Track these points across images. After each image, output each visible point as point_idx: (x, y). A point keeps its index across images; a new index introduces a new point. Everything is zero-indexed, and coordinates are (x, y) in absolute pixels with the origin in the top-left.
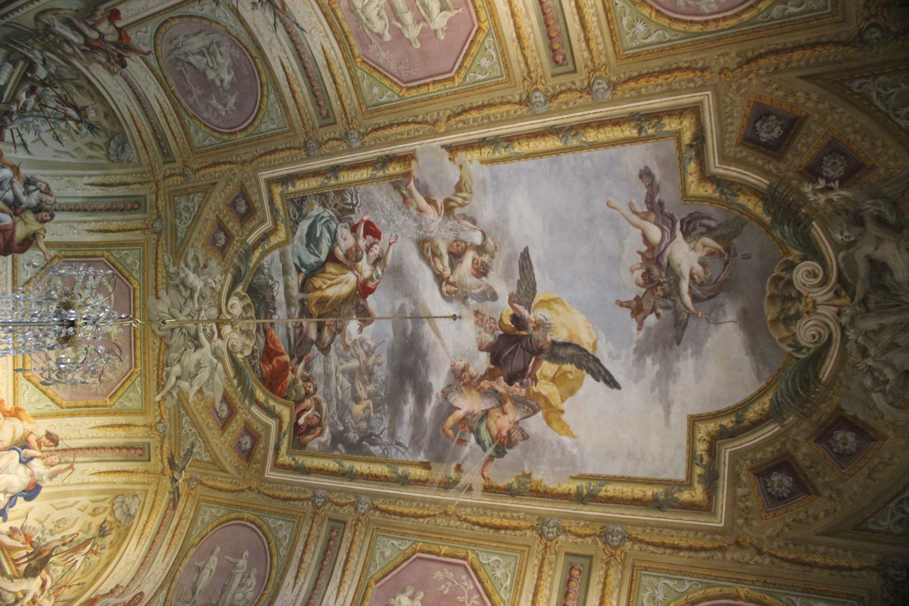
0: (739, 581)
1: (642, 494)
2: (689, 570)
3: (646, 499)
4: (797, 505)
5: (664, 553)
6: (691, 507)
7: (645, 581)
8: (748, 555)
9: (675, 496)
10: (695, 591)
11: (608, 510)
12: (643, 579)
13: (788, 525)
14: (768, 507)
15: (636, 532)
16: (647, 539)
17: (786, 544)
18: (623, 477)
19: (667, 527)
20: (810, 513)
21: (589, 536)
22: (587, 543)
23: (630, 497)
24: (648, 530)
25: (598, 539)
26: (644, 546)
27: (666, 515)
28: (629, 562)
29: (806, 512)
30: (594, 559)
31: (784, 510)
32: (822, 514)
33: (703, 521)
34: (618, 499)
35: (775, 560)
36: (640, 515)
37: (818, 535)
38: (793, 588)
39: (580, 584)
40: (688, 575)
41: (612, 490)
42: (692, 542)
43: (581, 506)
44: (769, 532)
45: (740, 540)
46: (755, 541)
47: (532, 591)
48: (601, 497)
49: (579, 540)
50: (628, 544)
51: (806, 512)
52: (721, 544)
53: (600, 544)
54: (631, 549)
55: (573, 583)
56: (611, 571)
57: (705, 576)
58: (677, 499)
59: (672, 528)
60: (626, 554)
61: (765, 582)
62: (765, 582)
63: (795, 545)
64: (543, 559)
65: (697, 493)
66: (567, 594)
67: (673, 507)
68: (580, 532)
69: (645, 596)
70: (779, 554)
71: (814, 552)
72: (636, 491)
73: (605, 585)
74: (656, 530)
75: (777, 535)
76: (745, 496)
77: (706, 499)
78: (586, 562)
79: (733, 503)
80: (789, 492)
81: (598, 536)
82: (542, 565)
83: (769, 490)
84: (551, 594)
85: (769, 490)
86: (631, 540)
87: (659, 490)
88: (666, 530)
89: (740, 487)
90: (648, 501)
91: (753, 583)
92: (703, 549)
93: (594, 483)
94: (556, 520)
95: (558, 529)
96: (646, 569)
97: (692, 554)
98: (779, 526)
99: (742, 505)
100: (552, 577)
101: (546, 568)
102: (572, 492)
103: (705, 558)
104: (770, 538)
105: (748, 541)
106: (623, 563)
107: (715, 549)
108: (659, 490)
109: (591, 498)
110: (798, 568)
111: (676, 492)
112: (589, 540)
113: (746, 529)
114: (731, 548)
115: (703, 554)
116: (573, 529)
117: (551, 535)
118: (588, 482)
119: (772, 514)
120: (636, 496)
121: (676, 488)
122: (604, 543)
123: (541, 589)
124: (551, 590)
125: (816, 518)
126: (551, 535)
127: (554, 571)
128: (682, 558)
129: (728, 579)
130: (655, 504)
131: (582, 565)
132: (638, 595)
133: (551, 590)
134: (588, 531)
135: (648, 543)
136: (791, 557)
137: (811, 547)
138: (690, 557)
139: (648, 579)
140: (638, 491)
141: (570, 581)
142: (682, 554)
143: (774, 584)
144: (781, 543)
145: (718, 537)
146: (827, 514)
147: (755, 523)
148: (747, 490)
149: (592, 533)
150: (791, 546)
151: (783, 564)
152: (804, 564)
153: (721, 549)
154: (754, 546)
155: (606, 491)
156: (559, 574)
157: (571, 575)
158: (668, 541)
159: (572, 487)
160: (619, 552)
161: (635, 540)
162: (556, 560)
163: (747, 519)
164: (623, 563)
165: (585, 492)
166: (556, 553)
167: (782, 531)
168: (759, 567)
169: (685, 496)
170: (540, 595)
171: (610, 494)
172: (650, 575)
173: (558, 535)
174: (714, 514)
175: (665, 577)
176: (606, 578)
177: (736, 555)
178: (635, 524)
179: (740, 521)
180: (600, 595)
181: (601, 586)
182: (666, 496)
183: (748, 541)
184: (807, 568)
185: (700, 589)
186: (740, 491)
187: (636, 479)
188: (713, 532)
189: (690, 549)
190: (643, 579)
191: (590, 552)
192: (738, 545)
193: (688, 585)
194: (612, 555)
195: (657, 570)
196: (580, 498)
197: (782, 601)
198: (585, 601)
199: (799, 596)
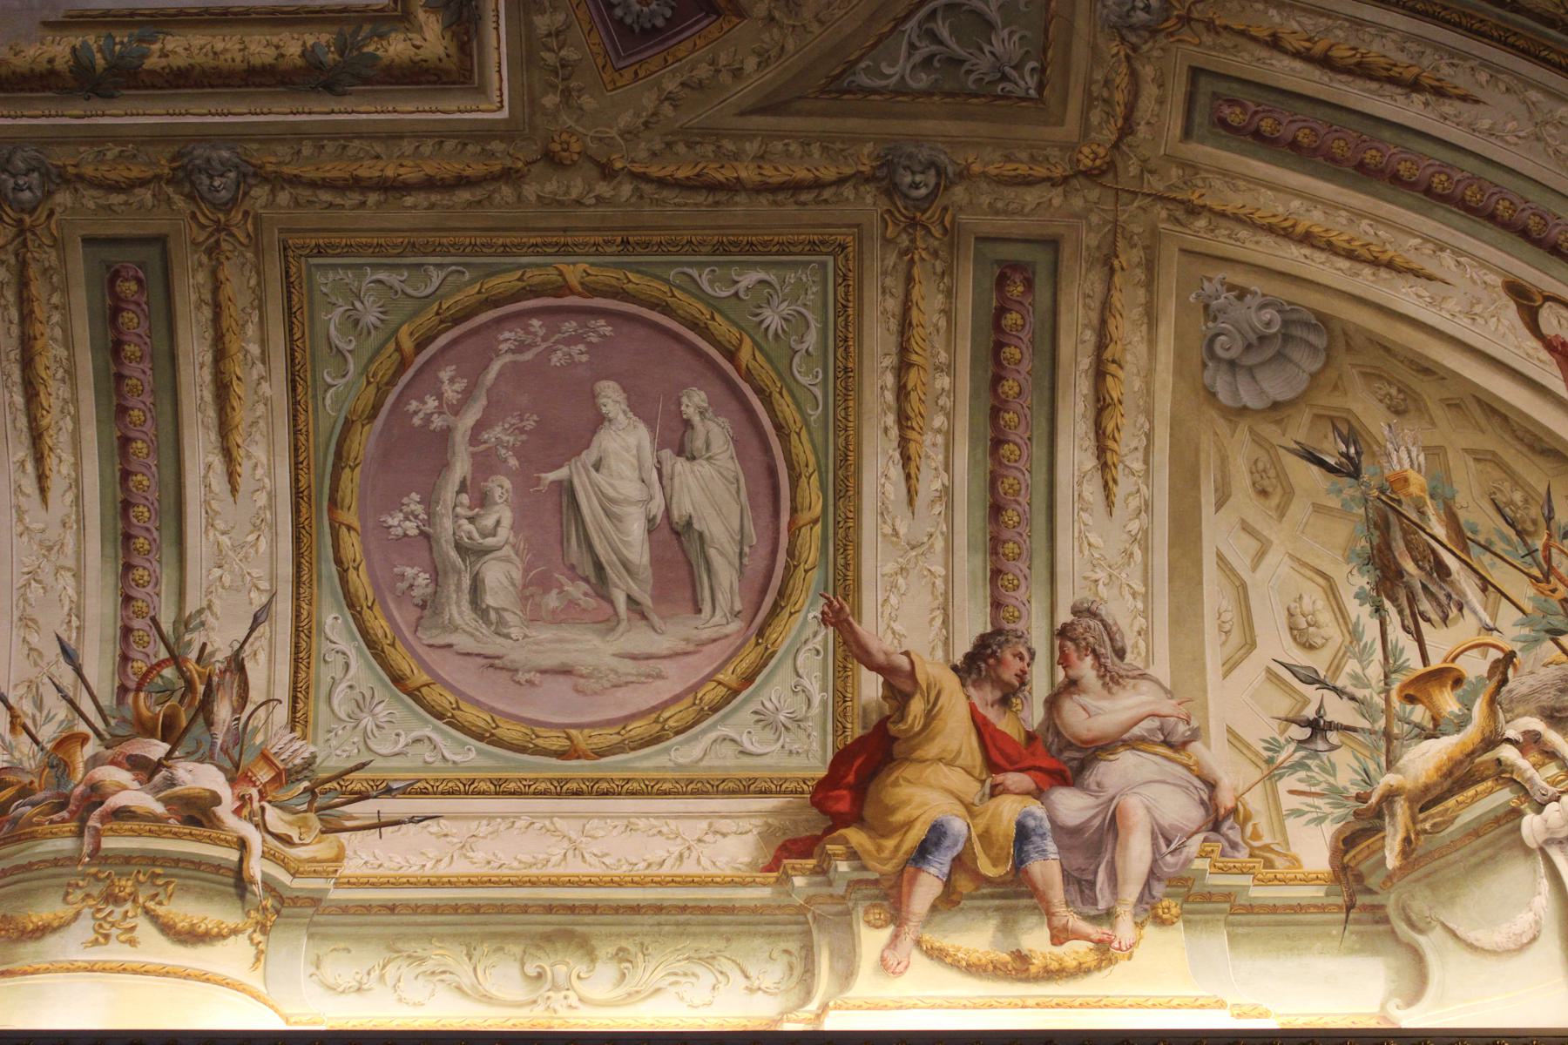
0: (563, 250)
1: (272, 52)
2: (433, 238)
3: (283, 64)
4: (689, 44)
5: (363, 204)
6: (416, 77)
7: (325, 281)
8: (579, 182)
9: (370, 49)
10: (459, 289)
11: (182, 106)
12: (319, 278)
13: (669, 98)
14: (619, 57)
15: (274, 158)
16: (310, 173)
17: (669, 145)
18: (206, 11)
19: (360, 136)
20: (723, 60)
21: (143, 183)
22: (141, 205)
23: (239, 64)
24: (307, 150)
25: (170, 190)
26: (305, 194)
27: (348, 103)
28: (272, 237)
29: (713, 63)
30: (171, 245)
31: (658, 60)
32: (751, 63)
33: (454, 110)
34: (204, 72)
35: (643, 186)
36: (279, 112)
37: (742, 114)
38: (692, 247)
39: (148, 317)
40: (433, 253)
41: (180, 48)
42: (430, 169)
43: (98, 105)
44: (625, 120)
45: (556, 147)
46: (593, 147)
47: (15, 354)
48: (152, 72)
49: (116, 199)
50: (260, 193)
51: (713, 63)
52: (508, 163)
53: (180, 202)
54: (272, 203)
55: (126, 316)
56: (227, 270)
57: (476, 250)
58: (374, 57)
59: (373, 137)
60: (257, 218)
61: (625, 242)
62: (625, 242)
63: (690, 145)
64: (23, 265)
65: (430, 38)
66: (117, 348)
67: (366, 81)
68: (113, 176)
69: (332, 321)
70: (654, 171)
71: (736, 157)
72: (253, 48)
73: (217, 308)
74: (330, 147)
75: (646, 124)
76: (558, 33)
77: (453, 50)
78: (153, 253)
79: (526, 56)
80: (669, 13)
81: (168, 182)
82: (23, 284)
83: (618, 12)
84: (71, 357)
85: (618, 12)
86: (266, 180)
87: (321, 38)
88: (357, 143)
89: (543, 12)
90: (296, 70)
91: (597, 249)
92: (462, 182)
93: (121, 36)
94: (30, 152)
95: (46, 175)
96: (320, 251)
97: (434, 198)
98: (649, 101)
99: (550, 58)
100: (65, 309)
101: (37, 288)
102: (60, 65)
103: (470, 204)
104: (629, 134)
105: (576, 147)
106: (255, 243)
107: (493, 178)
108: (321, 38)
109: (124, 78)
110: (700, 198)
111: (370, 38)
112: (146, 195)
113: (566, 119)
114: (535, 169)
115: (465, 195)
116: (88, 171)
117: (26, 195)
118: (104, 32)
119: (628, 74)
120: (256, 61)
121: (367, 28)
122: (190, 197)
123: (39, 344)
124: (68, 342)
125: (737, 73)
126: (27, 195)
127: (66, 290)
128: (414, 210)
129: (536, 249)
130: (315, 78)
131: (141, 265)
132: (312, 319)
133: (68, 342)
134: (135, 173)
135: (313, 184)
136: (680, 174)
137: (729, 145)
138: (432, 206)
139: (331, 276)
140: (259, 47)
141: (116, 311)
142: (409, 200)
143: (647, 245)
144: (658, 146)
145: (497, 146)
146: (763, 63)
147: (587, 101)
148: (560, 18)
149: (150, 174)
150: (681, 148)
151: (665, 193)
152: (713, 187)
153: (508, 175)
154: (590, 158)
155: (164, 55)
156: (80, 298)
157: (115, 296)
158: (366, 171)
159: (59, 50)
160: (237, 216)
161: (277, 181)
162: (63, 261)
163: (567, 94)
164: (255, 243)
165: (100, 62)
166: (58, 244)
167: (654, 114)
168: (609, 210)
169: (397, 47)
170: (40, 363)
171: (179, 61)
172: (334, 267)
173: (49, 194)
174: (481, 90)
175: (376, 267)
176: (217, 287)
177: (550, 187)
178: (270, 137)
179: (550, 100)
180: (209, 334)
181: (207, 312)
182: (342, 54)
183: (576, 147)
184: (722, 196)
185: (471, 282)
186: (543, 23)
187: (247, 12)
188: (482, 134)
189: (429, 184)
190: (319, 278)
191: (150, 230)
192: (552, 160)
193: (436, 277)
194: (220, 228)
195: (349, 250)
196: (85, 81)
197: (667, 281)
198: (173, 358)
199: (708, 264)
